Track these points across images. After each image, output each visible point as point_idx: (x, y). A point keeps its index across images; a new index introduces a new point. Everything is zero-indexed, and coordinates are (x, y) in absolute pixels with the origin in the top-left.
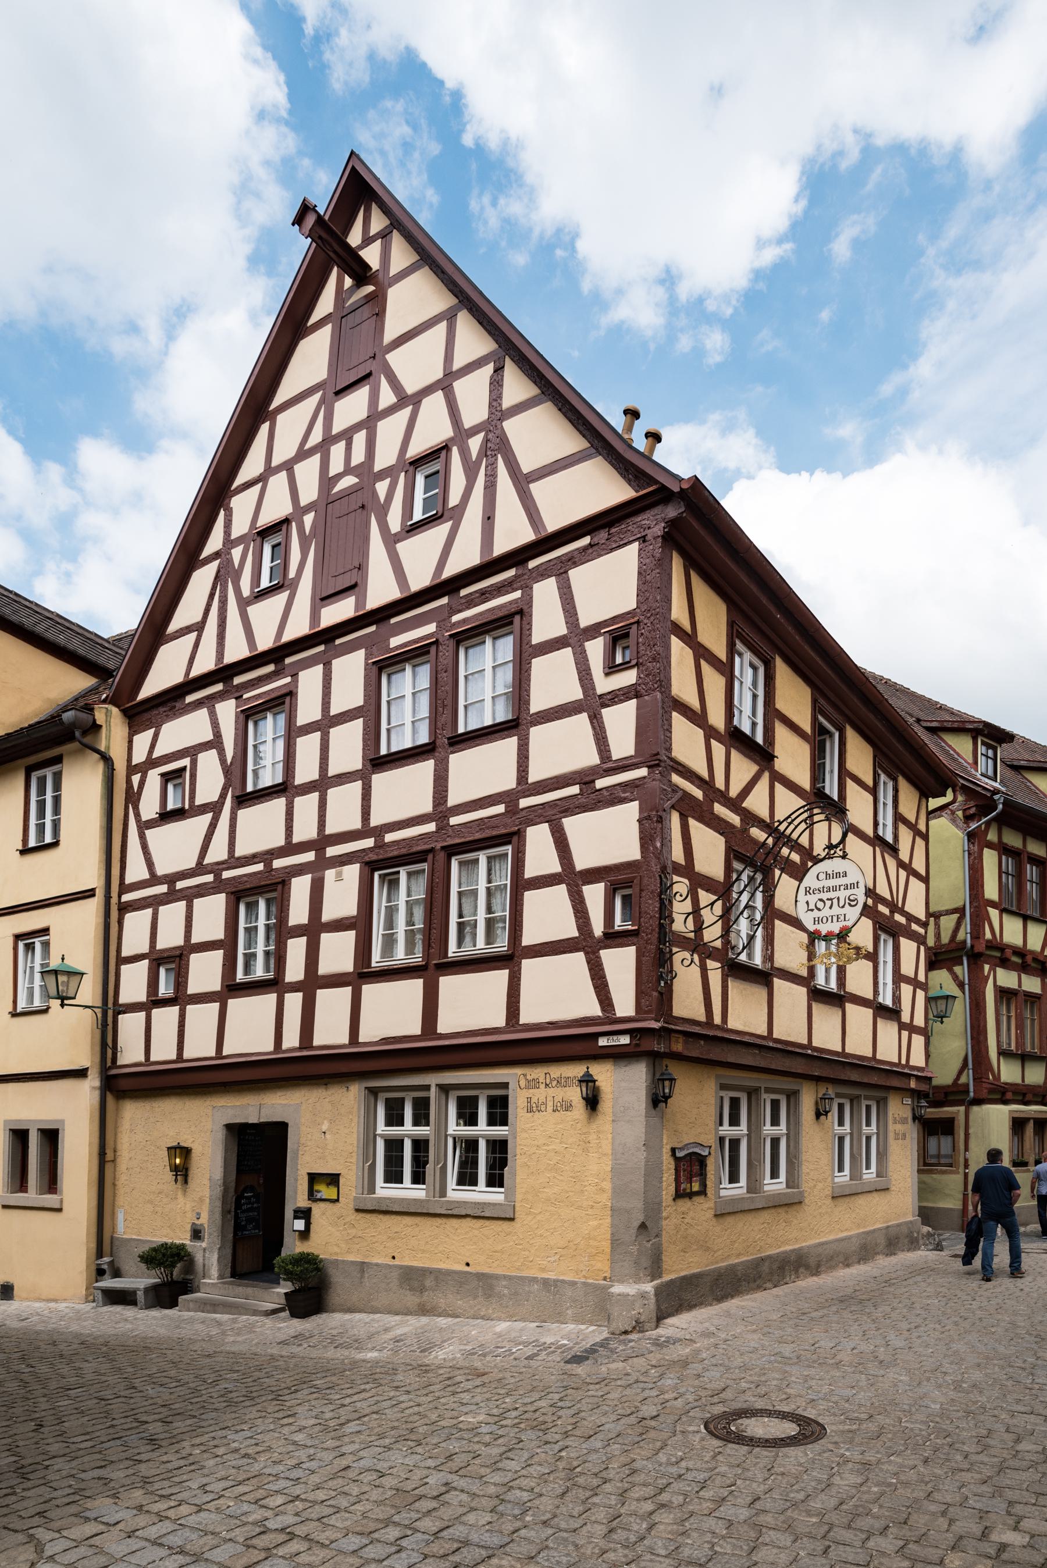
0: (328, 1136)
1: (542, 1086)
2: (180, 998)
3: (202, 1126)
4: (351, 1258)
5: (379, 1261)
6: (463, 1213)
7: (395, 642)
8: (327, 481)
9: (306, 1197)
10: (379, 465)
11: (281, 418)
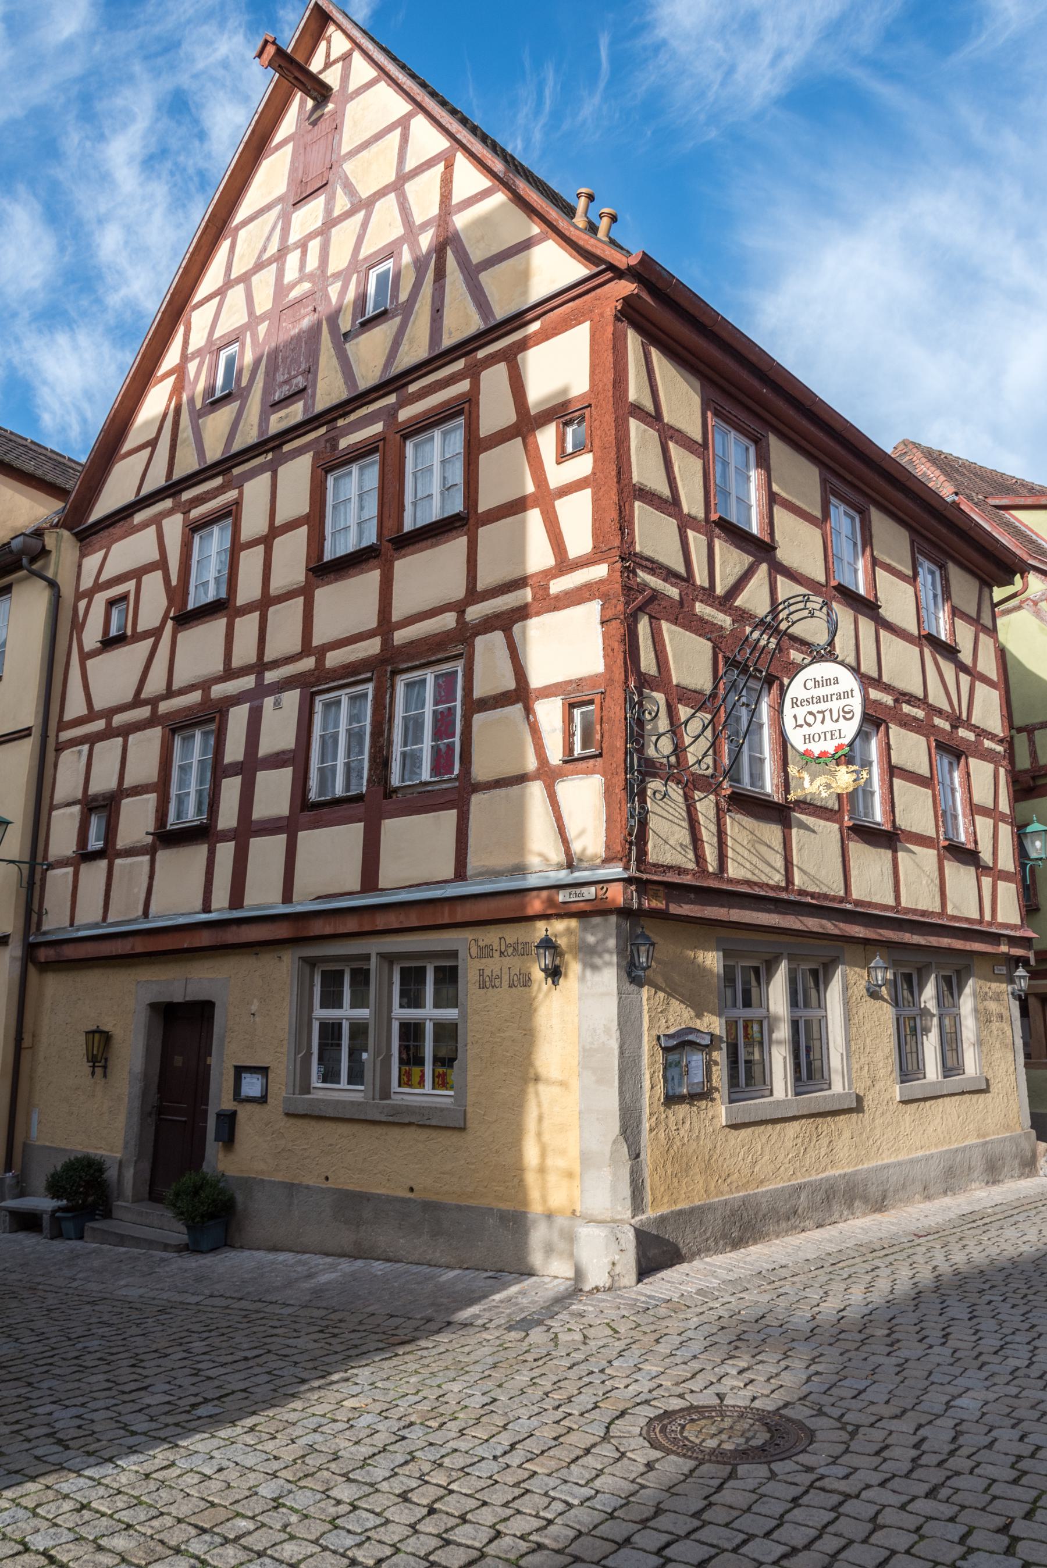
0: (257, 1019)
1: (497, 954)
2: (108, 852)
3: (121, 1003)
4: (278, 1178)
5: (311, 1183)
6: (406, 1121)
7: (343, 443)
8: (281, 289)
9: (231, 1097)
10: (333, 267)
11: (242, 234)
